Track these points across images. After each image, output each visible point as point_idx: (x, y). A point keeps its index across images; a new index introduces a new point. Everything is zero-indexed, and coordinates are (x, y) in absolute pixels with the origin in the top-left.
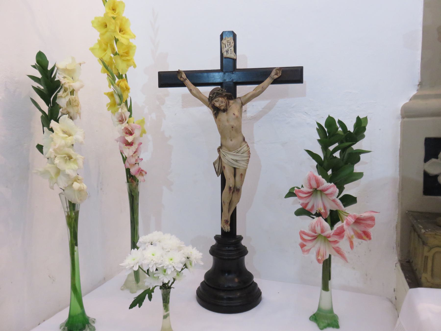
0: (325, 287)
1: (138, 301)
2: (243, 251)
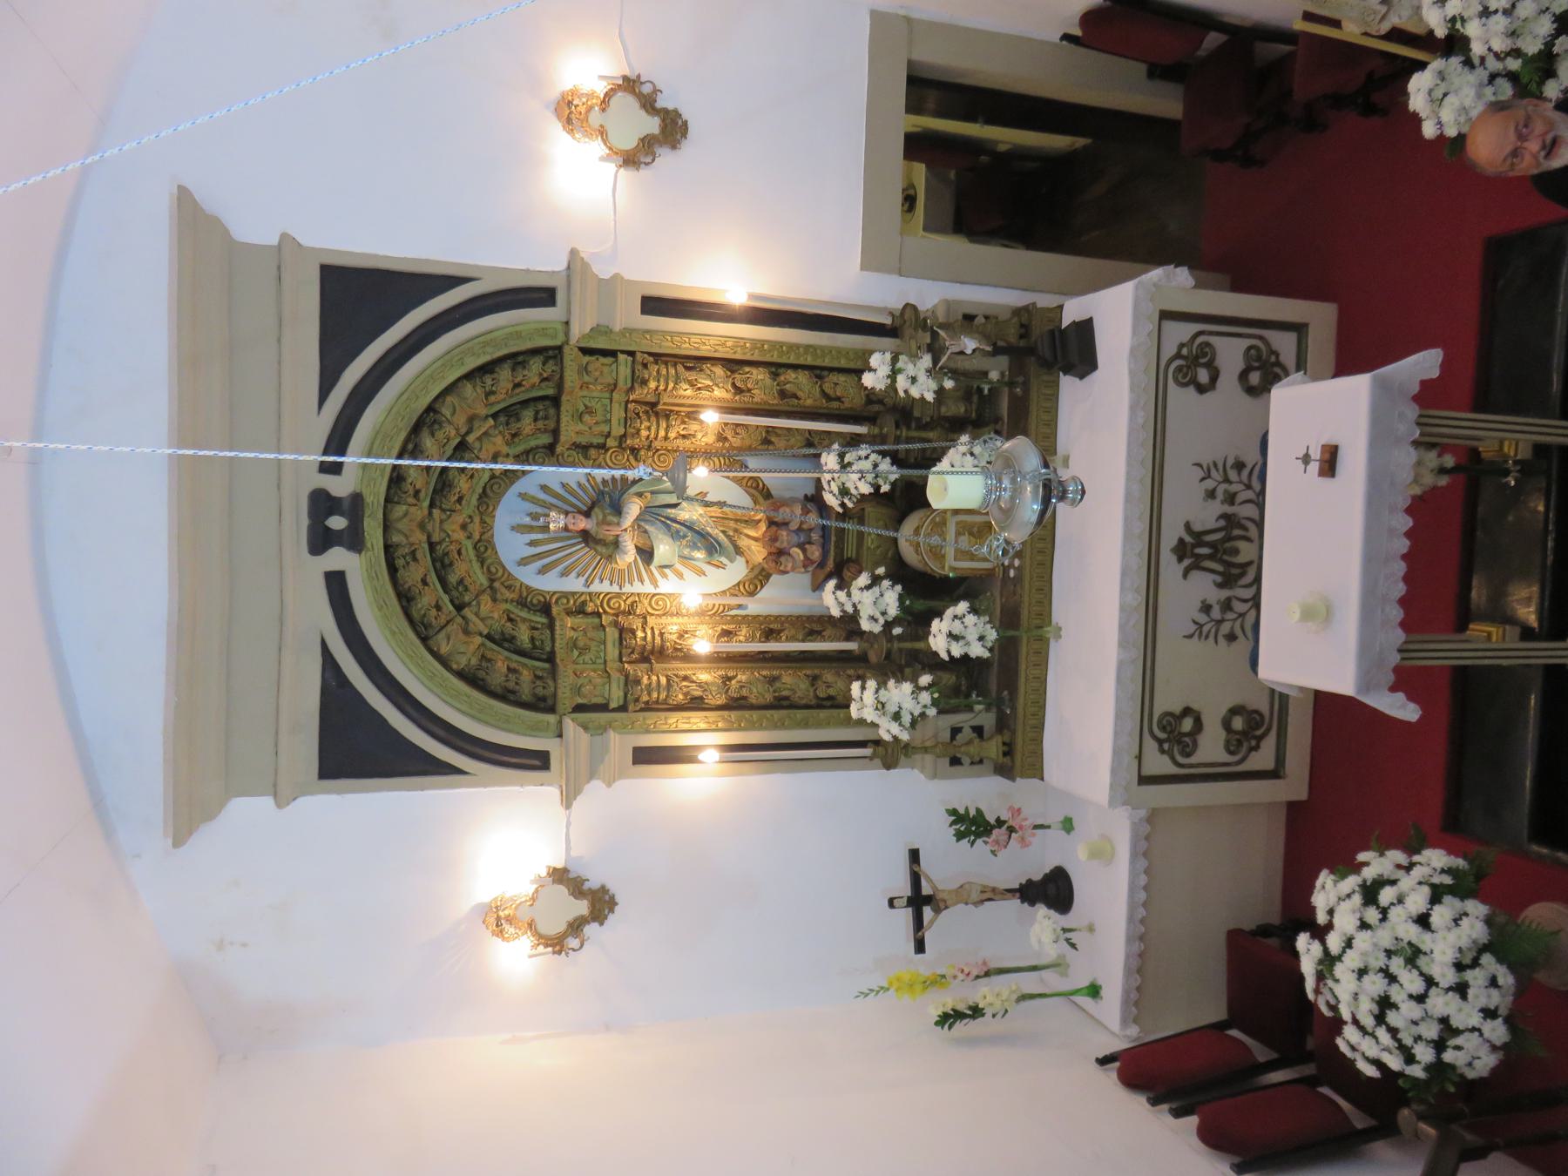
0: (1049, 827)
1: (1073, 946)
2: (1030, 881)
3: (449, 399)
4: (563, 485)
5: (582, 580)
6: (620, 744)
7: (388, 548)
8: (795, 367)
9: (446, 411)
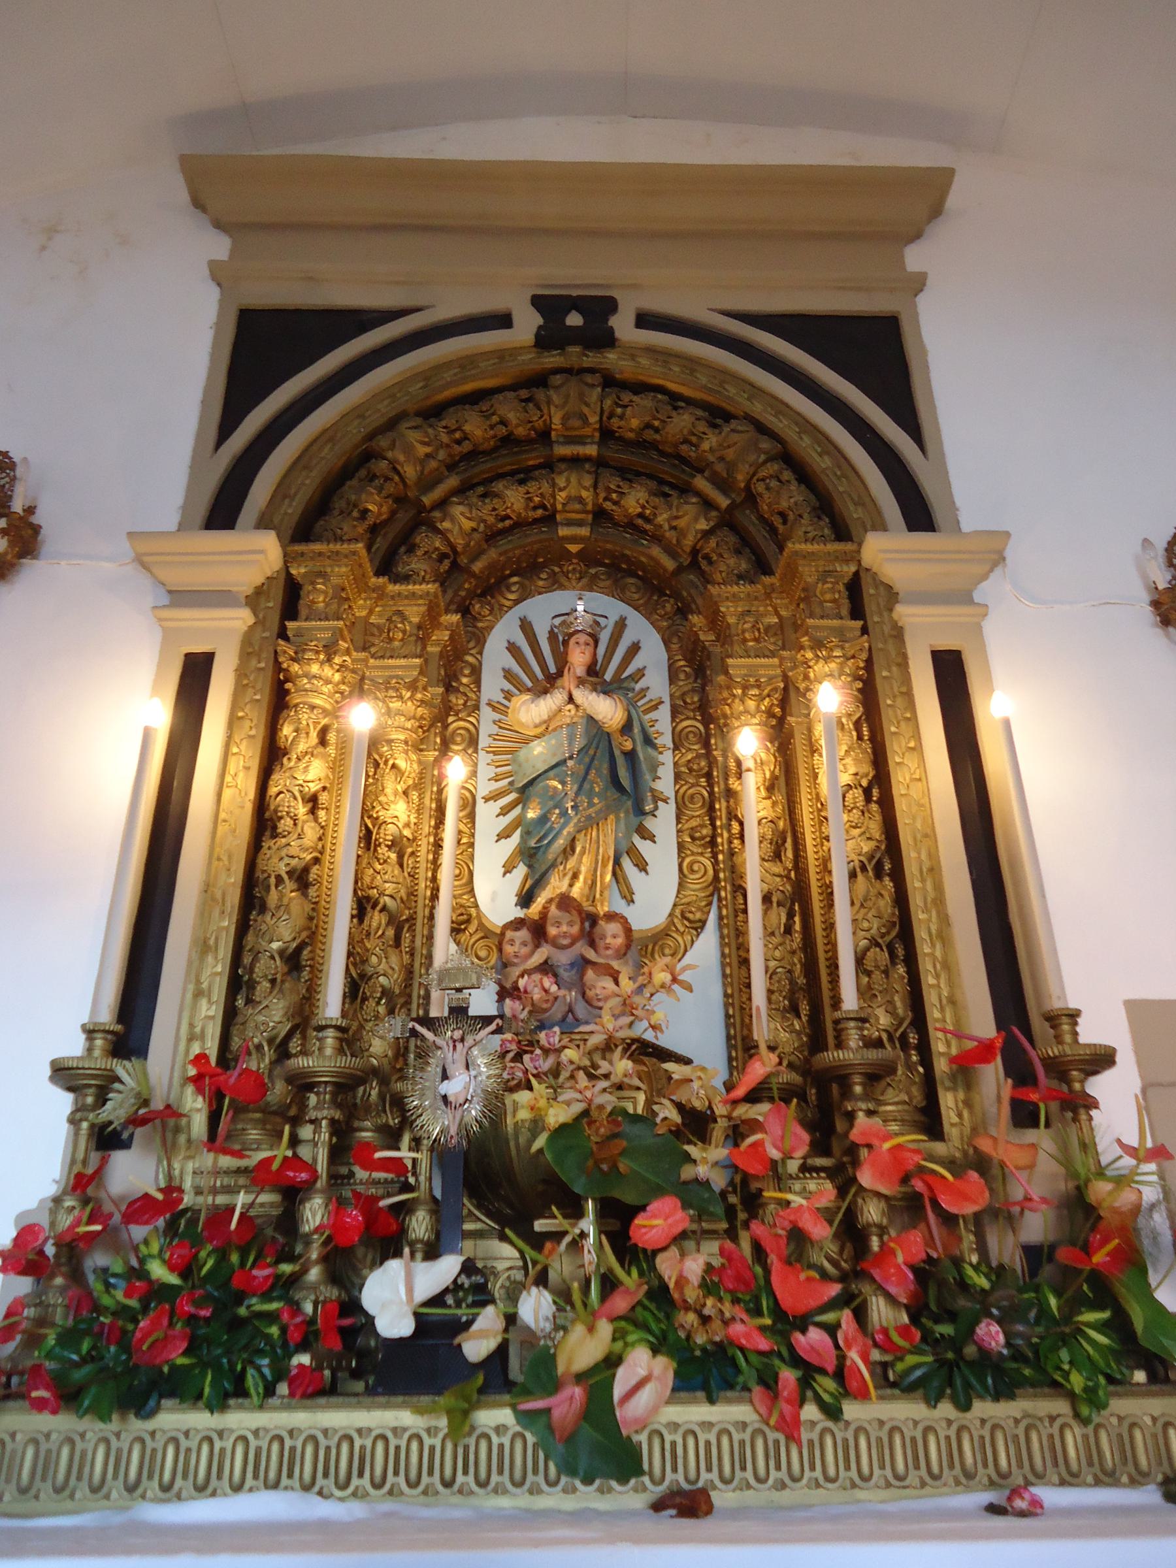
3: (750, 433)
4: (640, 673)
5: (499, 697)
6: (225, 631)
7: (540, 380)
8: (901, 899)
9: (734, 424)
